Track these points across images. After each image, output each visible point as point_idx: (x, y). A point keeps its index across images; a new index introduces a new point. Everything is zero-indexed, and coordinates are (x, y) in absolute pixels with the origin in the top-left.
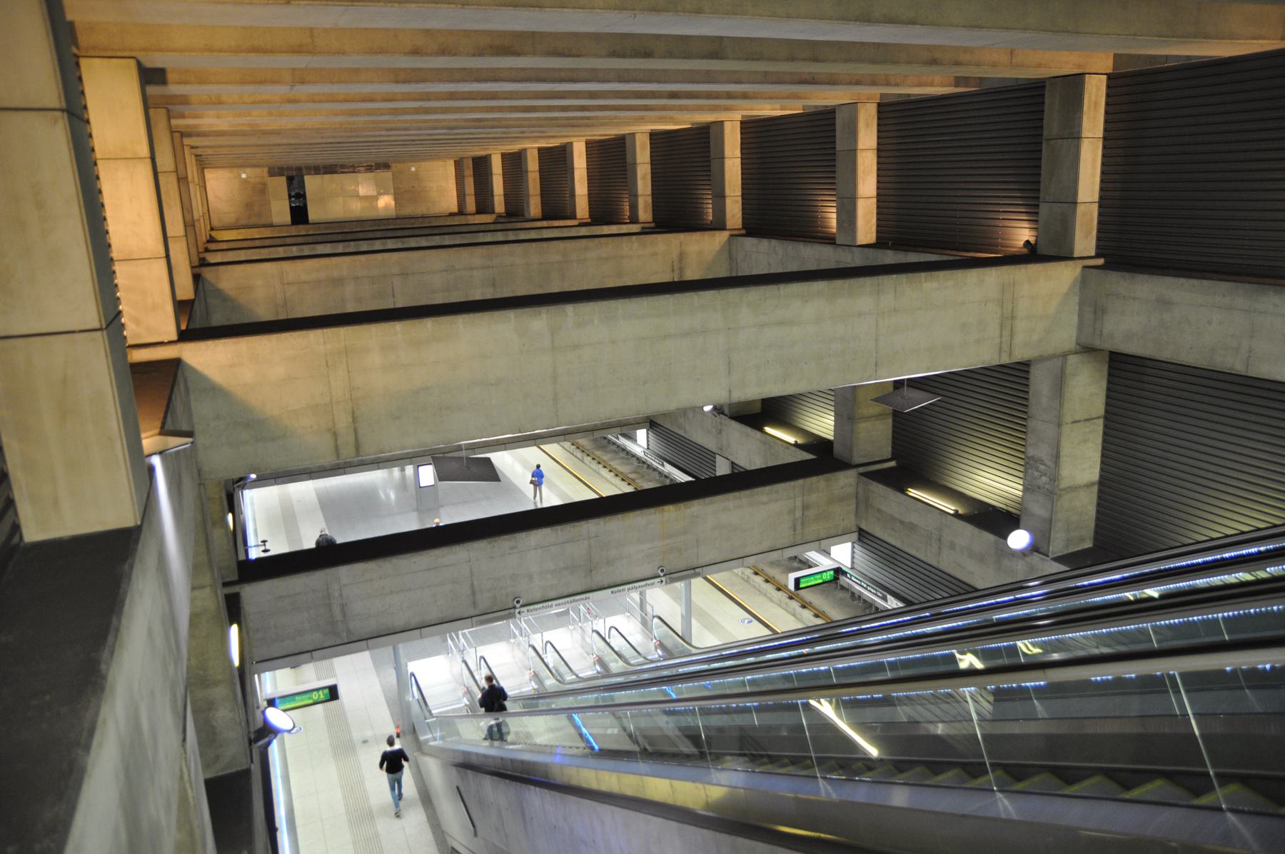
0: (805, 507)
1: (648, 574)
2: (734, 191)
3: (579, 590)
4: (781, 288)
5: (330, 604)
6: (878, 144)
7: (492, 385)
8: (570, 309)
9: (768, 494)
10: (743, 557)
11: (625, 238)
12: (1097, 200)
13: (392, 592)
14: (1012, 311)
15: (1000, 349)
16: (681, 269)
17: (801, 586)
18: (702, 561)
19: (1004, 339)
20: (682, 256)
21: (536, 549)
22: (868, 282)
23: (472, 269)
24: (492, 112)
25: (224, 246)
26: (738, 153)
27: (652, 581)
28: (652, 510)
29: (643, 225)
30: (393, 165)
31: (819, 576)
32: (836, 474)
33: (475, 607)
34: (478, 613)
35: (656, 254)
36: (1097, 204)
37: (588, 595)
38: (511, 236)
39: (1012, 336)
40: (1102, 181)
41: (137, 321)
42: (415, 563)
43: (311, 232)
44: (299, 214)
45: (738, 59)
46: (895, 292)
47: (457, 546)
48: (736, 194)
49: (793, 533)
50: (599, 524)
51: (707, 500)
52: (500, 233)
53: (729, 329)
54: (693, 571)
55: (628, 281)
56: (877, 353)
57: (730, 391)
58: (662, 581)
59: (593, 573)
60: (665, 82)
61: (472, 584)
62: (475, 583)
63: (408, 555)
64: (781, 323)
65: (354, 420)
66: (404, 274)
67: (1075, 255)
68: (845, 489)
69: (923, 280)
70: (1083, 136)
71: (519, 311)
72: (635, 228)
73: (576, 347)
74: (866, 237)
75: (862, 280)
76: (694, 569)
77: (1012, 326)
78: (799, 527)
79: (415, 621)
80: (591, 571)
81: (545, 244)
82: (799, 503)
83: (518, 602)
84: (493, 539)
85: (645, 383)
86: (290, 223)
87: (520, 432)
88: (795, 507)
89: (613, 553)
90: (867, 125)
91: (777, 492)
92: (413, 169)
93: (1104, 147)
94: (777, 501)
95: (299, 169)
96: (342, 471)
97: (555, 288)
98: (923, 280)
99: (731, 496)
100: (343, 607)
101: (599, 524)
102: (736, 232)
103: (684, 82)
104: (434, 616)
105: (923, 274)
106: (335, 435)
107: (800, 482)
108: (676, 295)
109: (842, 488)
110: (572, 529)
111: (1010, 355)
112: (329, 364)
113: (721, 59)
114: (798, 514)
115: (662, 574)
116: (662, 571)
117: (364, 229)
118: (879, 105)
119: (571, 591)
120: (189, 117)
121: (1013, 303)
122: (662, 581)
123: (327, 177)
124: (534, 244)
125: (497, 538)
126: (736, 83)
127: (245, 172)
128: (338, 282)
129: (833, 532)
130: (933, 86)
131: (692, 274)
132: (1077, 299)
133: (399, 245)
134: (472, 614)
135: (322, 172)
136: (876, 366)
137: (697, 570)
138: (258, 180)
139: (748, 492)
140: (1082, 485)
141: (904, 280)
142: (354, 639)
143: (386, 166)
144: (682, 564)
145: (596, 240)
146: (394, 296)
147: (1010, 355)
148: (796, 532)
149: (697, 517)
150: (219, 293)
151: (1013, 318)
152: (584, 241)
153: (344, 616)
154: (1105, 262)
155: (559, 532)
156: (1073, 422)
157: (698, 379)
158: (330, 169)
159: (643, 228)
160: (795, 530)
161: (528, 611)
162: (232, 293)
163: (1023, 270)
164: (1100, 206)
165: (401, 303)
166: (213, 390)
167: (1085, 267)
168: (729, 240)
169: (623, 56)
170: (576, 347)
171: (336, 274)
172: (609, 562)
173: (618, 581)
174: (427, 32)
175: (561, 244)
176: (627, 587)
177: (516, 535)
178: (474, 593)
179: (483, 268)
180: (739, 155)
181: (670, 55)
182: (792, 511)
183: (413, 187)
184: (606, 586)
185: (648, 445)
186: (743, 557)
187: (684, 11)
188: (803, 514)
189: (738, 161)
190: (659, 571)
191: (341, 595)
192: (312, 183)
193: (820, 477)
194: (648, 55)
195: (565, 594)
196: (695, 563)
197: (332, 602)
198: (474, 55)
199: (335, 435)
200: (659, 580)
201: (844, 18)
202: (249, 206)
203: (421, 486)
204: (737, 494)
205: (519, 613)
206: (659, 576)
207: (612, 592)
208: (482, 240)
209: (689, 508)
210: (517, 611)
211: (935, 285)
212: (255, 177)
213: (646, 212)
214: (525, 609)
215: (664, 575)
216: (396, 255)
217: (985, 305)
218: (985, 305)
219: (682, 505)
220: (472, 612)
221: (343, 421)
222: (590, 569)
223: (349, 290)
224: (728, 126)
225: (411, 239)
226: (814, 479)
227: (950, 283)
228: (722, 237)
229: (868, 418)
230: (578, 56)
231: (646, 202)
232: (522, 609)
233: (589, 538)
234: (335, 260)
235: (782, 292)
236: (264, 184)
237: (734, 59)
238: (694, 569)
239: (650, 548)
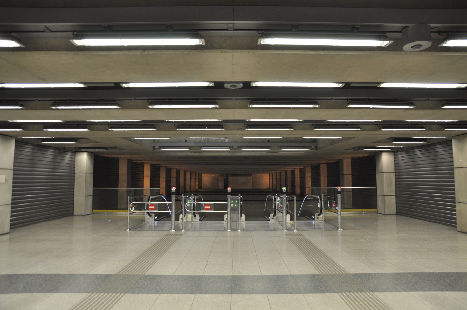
26: (299, 176)
92: (258, 176)
93: (327, 178)
123: (235, 177)
127: (213, 175)
158: (236, 175)
180: (299, 177)
189: (299, 178)
224: (296, 170)
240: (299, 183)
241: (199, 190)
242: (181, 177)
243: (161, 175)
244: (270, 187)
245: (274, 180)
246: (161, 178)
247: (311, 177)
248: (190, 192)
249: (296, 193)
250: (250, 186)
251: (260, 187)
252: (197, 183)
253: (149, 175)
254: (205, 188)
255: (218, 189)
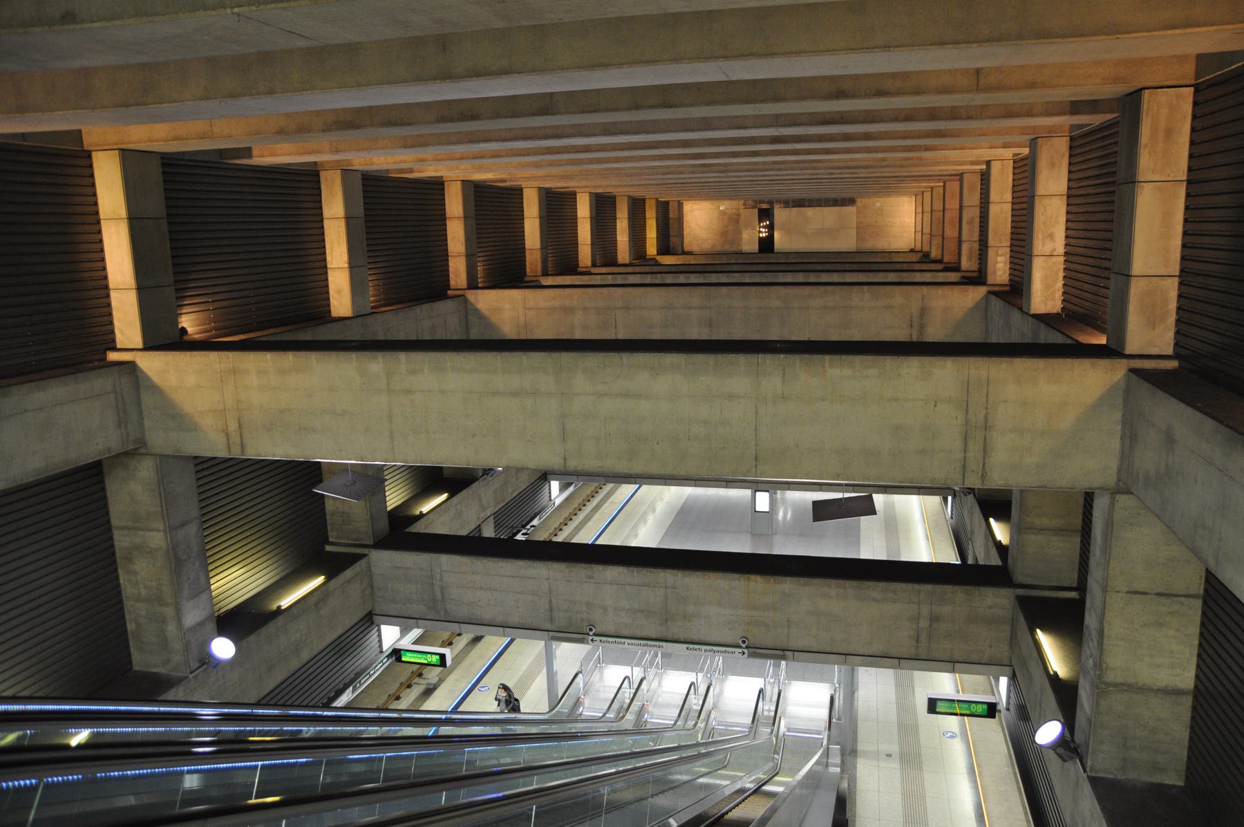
0: (934, 619)
1: (729, 640)
2: (1000, 241)
3: (654, 636)
4: (624, 356)
5: (433, 583)
6: (1069, 188)
7: (339, 415)
8: (402, 356)
9: (882, 591)
10: (846, 655)
11: (856, 288)
12: (1177, 274)
13: (481, 588)
14: (986, 418)
15: (964, 467)
16: (922, 327)
17: (938, 710)
18: (794, 644)
19: (971, 455)
20: (923, 311)
21: (611, 584)
22: (741, 359)
23: (690, 308)
24: (660, 160)
25: (666, 269)
26: (1008, 197)
27: (733, 650)
28: (736, 576)
29: (963, 274)
30: (860, 202)
31: (966, 706)
32: (983, 589)
33: (552, 623)
34: (554, 629)
35: (891, 307)
36: (1177, 279)
37: (661, 644)
38: (812, 278)
39: (986, 450)
40: (1184, 246)
41: (122, 333)
42: (501, 567)
43: (739, 262)
44: (766, 245)
45: (572, 113)
46: (784, 375)
47: (538, 562)
48: (1004, 244)
49: (916, 644)
50: (677, 576)
51: (802, 580)
52: (801, 273)
53: (563, 394)
54: (781, 653)
55: (856, 335)
56: (756, 445)
57: (565, 459)
58: (744, 653)
59: (669, 623)
60: (654, 132)
61: (550, 601)
62: (553, 599)
63: (496, 559)
64: (627, 395)
65: (240, 426)
66: (626, 308)
67: (1127, 352)
68: (994, 610)
69: (827, 364)
70: (1140, 178)
71: (359, 354)
72: (953, 277)
73: (408, 392)
74: (1046, 304)
75: (732, 357)
76: (783, 650)
77: (985, 438)
78: (923, 638)
79: (500, 619)
80: (666, 620)
81: (765, 289)
82: (925, 611)
83: (591, 630)
84: (571, 564)
85: (474, 436)
86: (757, 251)
87: (362, 461)
88: (919, 615)
89: (691, 609)
90: (1053, 165)
91: (895, 592)
92: (878, 205)
94: (894, 601)
95: (771, 203)
96: (633, 480)
97: (773, 335)
98: (827, 364)
99: (833, 582)
100: (442, 589)
101: (677, 576)
102: (996, 289)
103: (677, 131)
104: (515, 619)
105: (827, 357)
106: (227, 435)
107: (929, 587)
108: (504, 354)
109: (990, 607)
110: (648, 574)
111: (983, 477)
112: (223, 379)
113: (552, 114)
114: (924, 624)
115: (744, 646)
116: (744, 642)
117: (788, 261)
118: (1072, 139)
119: (645, 633)
120: (416, 172)
121: (987, 408)
122: (744, 653)
123: (795, 210)
124: (754, 288)
125: (575, 564)
126: (739, 128)
128: (569, 310)
129: (974, 657)
130: (1032, 116)
131: (935, 333)
132: (1118, 415)
133: (702, 280)
134: (549, 628)
135: (790, 205)
136: (756, 460)
137: (786, 653)
138: (734, 211)
139: (854, 583)
140: (1156, 688)
141: (798, 362)
142: (450, 619)
143: (851, 202)
144: (770, 642)
145: (822, 288)
146: (616, 327)
147: (983, 477)
148: (920, 644)
149: (790, 595)
150: (477, 310)
151: (987, 427)
152: (808, 289)
153: (443, 597)
154: (1180, 366)
155: (635, 573)
156: (1128, 592)
157: (529, 441)
158: (800, 203)
159: (963, 277)
160: (917, 641)
161: (601, 641)
162: (486, 313)
163: (1004, 366)
164: (1181, 284)
165: (622, 335)
166: (154, 389)
167: (1133, 371)
168: (986, 295)
169: (452, 120)
170: (408, 392)
171: (567, 303)
172: (686, 617)
173: (695, 637)
174: (288, 115)
175: (782, 290)
176: (704, 647)
177: (593, 566)
178: (551, 610)
179: (701, 308)
180: (1010, 199)
181: (497, 115)
182: (916, 619)
183: (877, 222)
184: (682, 640)
185: (952, 514)
186: (846, 655)
187: (258, 94)
188: (930, 626)
189: (1008, 208)
190: (741, 643)
191: (441, 579)
192: (780, 214)
193: (956, 587)
194: (474, 117)
195: (639, 636)
196: (785, 646)
197: (434, 582)
198: (324, 131)
199: (227, 435)
200: (740, 650)
201: (418, 79)
202: (724, 234)
203: (757, 510)
204: (841, 582)
205: (592, 640)
206: (741, 647)
207: (687, 648)
208: (782, 280)
209: (780, 584)
210: (590, 638)
211: (846, 372)
212: (732, 209)
213: (970, 259)
214: (598, 638)
215: (747, 647)
216: (620, 291)
217: (935, 406)
218: (935, 406)
219: (772, 579)
220: (549, 627)
221: (233, 426)
222: (666, 617)
223: (578, 317)
224: (996, 168)
225: (713, 275)
226: (948, 588)
227: (872, 372)
228: (976, 294)
229: (1041, 530)
230: (410, 124)
231: (971, 249)
232: (595, 638)
233: (666, 587)
234: (568, 291)
235: (625, 361)
236: (739, 215)
237: (567, 113)
238: (783, 650)
239: (732, 615)
240: (1009, 230)
241: (659, 258)
242: (526, 213)
243: (327, 213)
244: (915, 246)
245: (927, 217)
246: (326, 223)
247: (1069, 196)
248: (594, 270)
249: (990, 280)
250: (846, 243)
251: (882, 244)
252: (651, 234)
253: (123, 213)
254: (695, 248)
255: (741, 253)
